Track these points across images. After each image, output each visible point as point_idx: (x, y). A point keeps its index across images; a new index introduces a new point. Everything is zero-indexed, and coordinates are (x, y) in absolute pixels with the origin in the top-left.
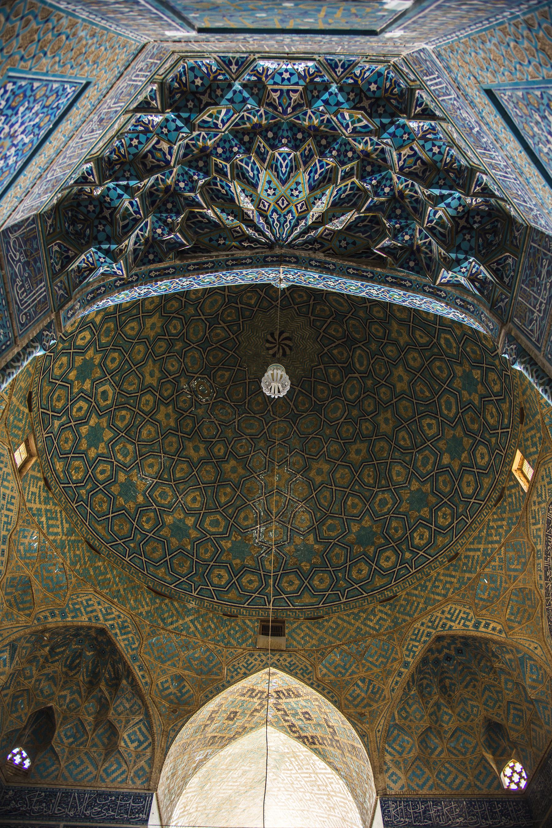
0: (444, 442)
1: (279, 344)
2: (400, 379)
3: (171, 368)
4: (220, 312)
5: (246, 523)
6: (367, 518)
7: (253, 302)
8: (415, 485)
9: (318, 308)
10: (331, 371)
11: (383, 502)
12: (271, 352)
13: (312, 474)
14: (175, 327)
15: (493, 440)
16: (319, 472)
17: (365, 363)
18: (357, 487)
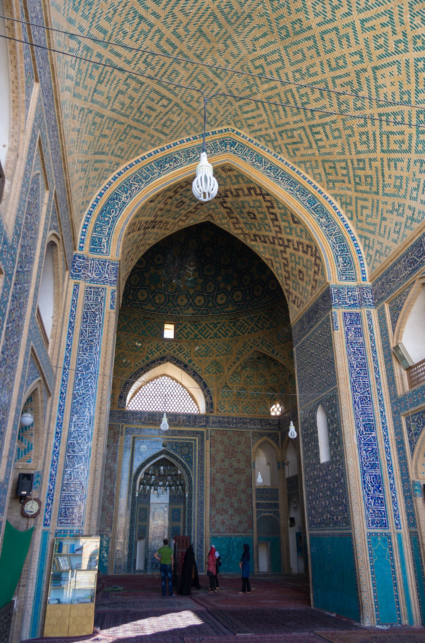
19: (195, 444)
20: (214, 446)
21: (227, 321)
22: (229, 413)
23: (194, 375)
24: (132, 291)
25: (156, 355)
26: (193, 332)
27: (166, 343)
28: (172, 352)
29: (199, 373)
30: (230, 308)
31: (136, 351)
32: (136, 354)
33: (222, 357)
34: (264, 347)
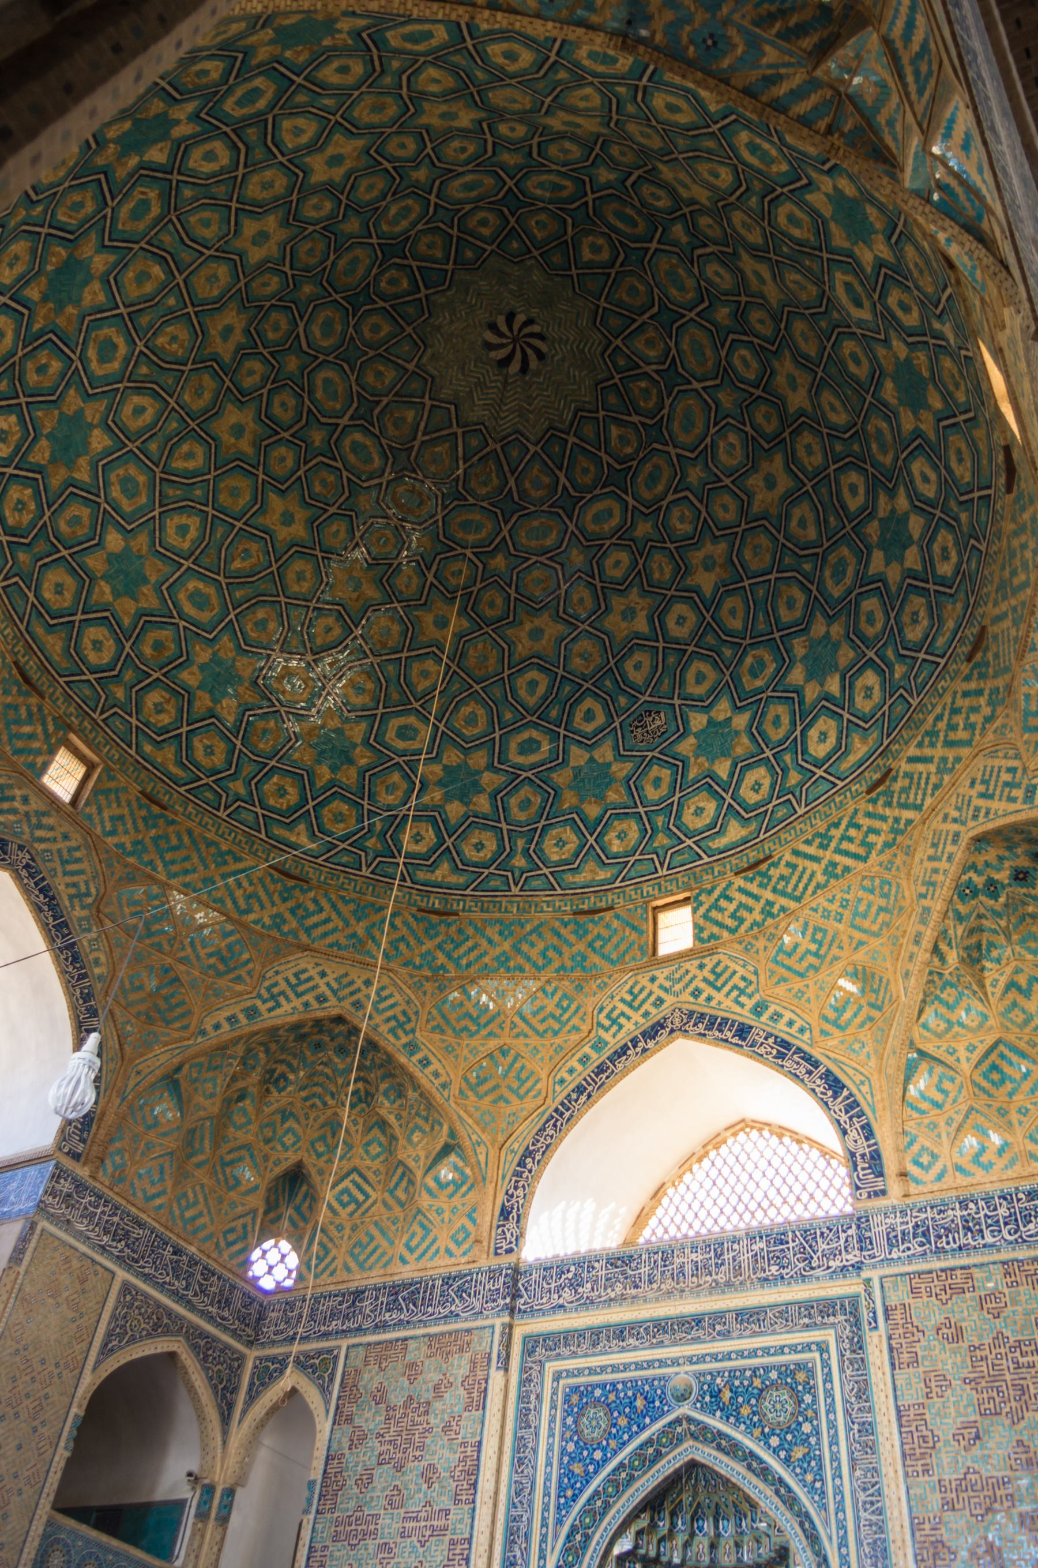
0: (145, 548)
1: (515, 341)
2: (288, 519)
3: (722, 271)
4: (667, 402)
5: (335, 64)
6: (101, 298)
7: (615, 431)
8: (99, 440)
9: (496, 481)
10: (390, 375)
11: (107, 349)
12: (521, 318)
13: (271, 222)
14: (745, 362)
15: (120, 693)
16: (262, 237)
17: (352, 458)
18: (172, 301)
19: (826, 1364)
20: (915, 1361)
21: (864, 806)
22: (961, 1180)
23: (781, 1056)
24: (520, 843)
25: (628, 1026)
26: (757, 898)
27: (661, 974)
28: (686, 997)
29: (802, 1042)
30: (860, 748)
31: (556, 1033)
32: (558, 1041)
33: (875, 943)
34: (995, 805)
